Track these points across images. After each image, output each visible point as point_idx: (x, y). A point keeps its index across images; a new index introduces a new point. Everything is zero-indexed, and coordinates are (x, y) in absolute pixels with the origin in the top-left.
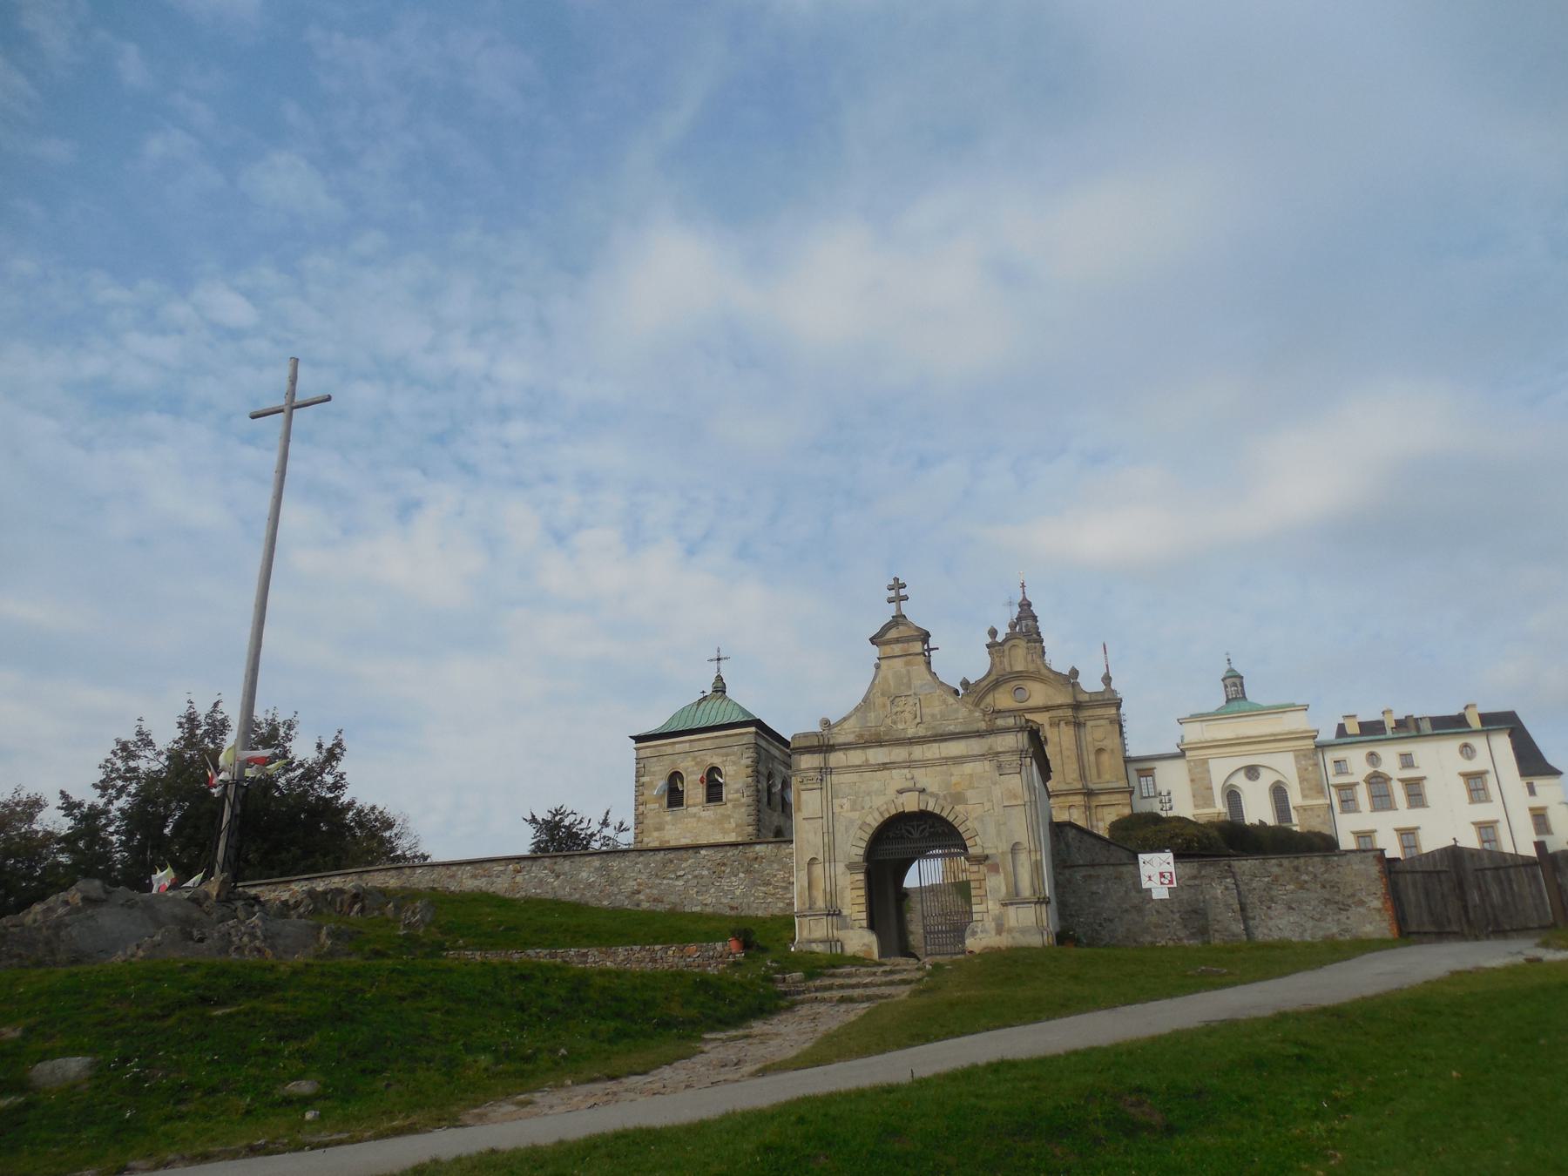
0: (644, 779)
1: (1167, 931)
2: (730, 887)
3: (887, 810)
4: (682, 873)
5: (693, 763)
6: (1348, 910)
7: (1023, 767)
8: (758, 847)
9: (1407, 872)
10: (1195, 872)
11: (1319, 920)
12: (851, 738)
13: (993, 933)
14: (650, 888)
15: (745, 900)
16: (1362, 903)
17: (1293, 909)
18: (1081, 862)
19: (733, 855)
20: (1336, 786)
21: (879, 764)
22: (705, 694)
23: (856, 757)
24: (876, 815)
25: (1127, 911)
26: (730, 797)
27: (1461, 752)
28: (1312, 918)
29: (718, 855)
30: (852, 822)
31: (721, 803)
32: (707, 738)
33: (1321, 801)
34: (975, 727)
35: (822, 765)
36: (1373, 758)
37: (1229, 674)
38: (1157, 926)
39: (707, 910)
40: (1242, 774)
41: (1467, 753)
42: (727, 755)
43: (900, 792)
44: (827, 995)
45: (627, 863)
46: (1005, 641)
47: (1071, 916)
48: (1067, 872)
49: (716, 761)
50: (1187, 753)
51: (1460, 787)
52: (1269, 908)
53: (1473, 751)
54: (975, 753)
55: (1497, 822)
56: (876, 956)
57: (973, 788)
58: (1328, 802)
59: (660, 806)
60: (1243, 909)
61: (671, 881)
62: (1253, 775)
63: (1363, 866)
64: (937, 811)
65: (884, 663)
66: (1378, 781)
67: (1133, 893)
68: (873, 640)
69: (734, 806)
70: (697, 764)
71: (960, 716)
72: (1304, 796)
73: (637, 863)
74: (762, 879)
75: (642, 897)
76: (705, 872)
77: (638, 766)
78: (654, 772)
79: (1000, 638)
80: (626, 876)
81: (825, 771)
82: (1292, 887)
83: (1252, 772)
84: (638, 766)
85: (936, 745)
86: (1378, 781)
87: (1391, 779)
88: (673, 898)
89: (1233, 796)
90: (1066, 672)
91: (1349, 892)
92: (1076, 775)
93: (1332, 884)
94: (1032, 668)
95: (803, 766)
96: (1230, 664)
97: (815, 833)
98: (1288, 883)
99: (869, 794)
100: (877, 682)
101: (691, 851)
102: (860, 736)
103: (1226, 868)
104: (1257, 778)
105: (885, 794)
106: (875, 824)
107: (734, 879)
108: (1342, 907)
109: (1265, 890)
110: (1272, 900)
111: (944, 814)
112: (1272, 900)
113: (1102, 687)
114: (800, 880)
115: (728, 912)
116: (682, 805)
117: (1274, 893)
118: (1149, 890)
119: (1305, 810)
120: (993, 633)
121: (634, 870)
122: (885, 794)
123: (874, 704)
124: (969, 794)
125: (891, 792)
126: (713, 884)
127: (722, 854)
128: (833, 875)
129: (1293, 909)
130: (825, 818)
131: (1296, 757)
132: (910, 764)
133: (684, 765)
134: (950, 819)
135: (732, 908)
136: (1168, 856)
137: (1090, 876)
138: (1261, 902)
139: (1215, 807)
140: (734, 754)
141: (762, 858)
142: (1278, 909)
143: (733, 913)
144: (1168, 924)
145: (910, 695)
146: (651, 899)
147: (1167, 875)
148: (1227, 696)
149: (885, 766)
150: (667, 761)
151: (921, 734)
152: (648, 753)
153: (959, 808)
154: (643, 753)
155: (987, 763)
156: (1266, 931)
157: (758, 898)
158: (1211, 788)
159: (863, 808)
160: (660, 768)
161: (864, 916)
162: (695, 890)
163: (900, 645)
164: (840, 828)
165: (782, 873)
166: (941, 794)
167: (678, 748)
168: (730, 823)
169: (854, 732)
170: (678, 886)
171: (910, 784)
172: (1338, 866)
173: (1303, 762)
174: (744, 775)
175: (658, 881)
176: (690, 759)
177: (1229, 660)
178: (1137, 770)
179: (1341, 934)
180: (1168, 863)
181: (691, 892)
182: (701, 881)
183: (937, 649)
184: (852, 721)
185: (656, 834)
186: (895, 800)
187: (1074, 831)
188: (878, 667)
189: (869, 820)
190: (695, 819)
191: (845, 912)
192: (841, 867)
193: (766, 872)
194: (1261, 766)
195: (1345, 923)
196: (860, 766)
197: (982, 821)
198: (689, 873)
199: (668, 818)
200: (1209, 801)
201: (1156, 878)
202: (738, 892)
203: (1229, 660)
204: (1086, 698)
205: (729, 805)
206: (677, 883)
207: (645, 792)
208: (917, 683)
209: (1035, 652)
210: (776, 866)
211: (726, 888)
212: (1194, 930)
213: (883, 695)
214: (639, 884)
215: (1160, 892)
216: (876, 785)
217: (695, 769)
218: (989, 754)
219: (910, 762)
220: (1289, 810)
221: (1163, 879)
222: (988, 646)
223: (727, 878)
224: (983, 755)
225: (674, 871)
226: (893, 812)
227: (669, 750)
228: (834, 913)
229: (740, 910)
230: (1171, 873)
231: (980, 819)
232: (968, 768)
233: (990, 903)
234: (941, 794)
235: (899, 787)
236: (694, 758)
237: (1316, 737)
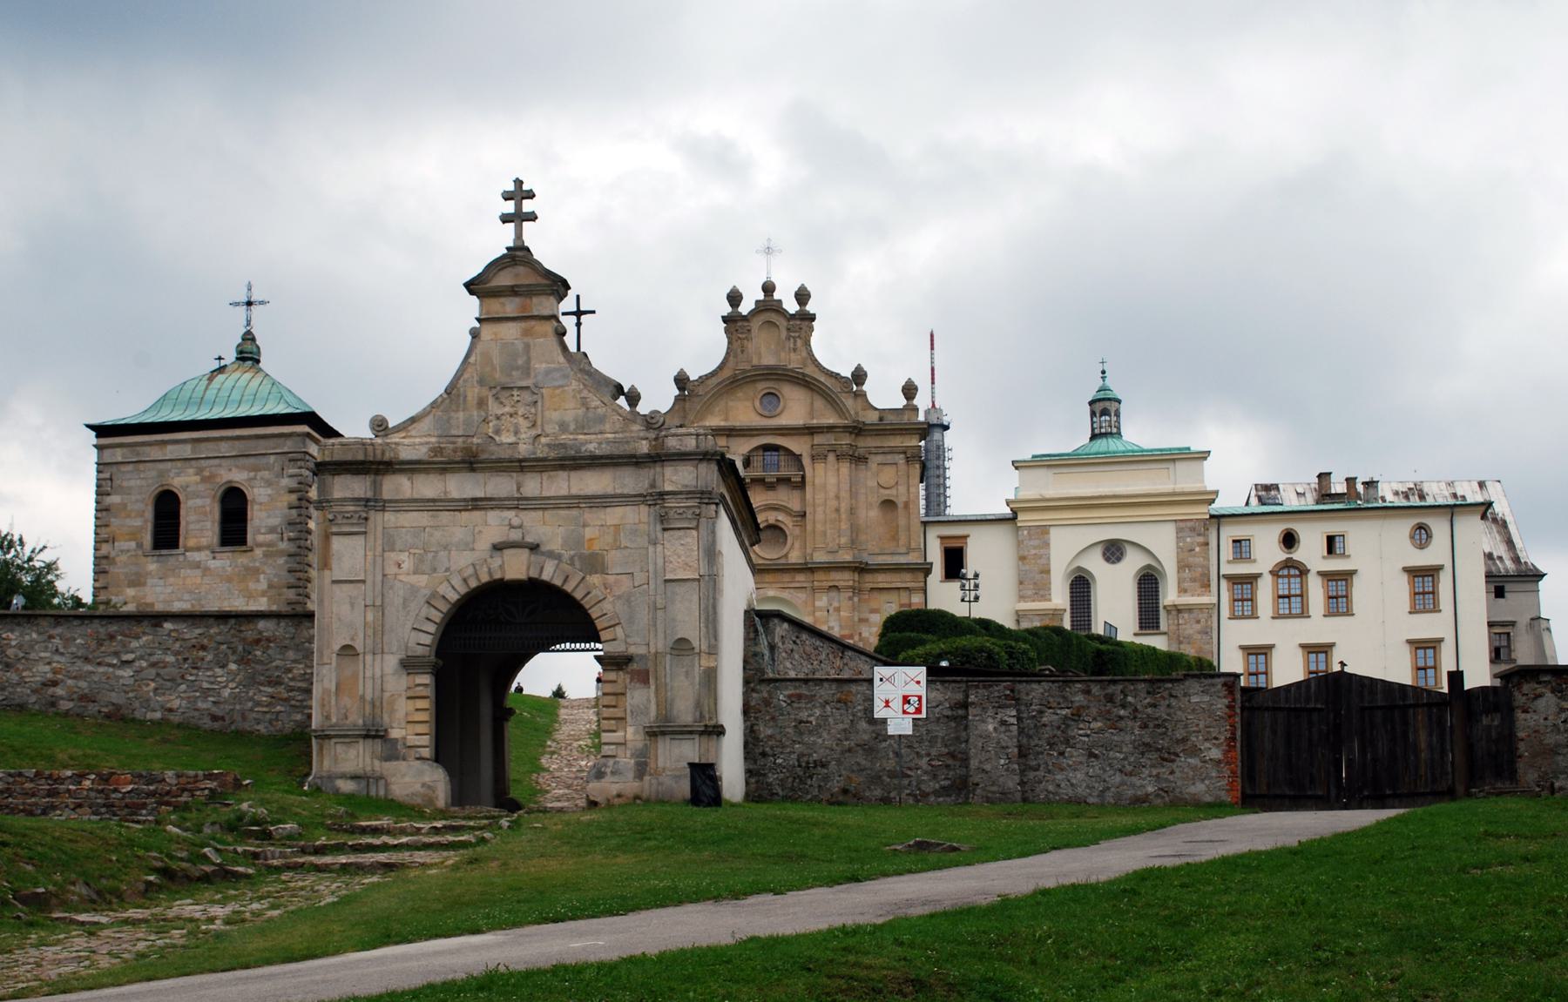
0: (115, 499)
1: (906, 782)
2: (212, 683)
3: (476, 575)
4: (130, 657)
5: (198, 478)
6: (1173, 761)
7: (703, 520)
8: (262, 624)
9: (1267, 709)
10: (960, 696)
11: (1131, 774)
12: (420, 453)
13: (631, 775)
14: (75, 678)
15: (238, 707)
16: (1195, 751)
17: (1096, 756)
18: (792, 674)
19: (220, 634)
20: (1229, 578)
21: (465, 500)
23: (428, 486)
24: (457, 582)
25: (850, 750)
26: (261, 538)
27: (1412, 537)
28: (1121, 771)
29: (192, 633)
30: (414, 590)
31: (244, 548)
32: (221, 439)
33: (1205, 600)
34: (628, 449)
35: (369, 495)
36: (1289, 540)
37: (1101, 394)
38: (892, 775)
39: (172, 718)
40: (1098, 552)
41: (1421, 539)
42: (256, 469)
43: (498, 548)
44: (327, 859)
45: (34, 636)
46: (753, 313)
47: (764, 754)
48: (764, 690)
51: (1401, 589)
52: (1062, 754)
53: (1429, 536)
54: (626, 491)
55: (1440, 641)
56: (441, 803)
57: (619, 548)
58: (1215, 600)
59: (140, 546)
60: (1023, 753)
61: (111, 670)
62: (1113, 554)
63: (1206, 698)
64: (558, 582)
65: (488, 332)
66: (1291, 569)
67: (863, 725)
68: (472, 286)
69: (266, 555)
70: (204, 480)
71: (607, 427)
72: (1182, 590)
73: (51, 637)
74: (268, 673)
75: (59, 691)
76: (170, 659)
77: (102, 476)
78: (130, 488)
79: (746, 307)
80: (33, 656)
81: (373, 503)
82: (1099, 724)
83: (1114, 551)
84: (102, 476)
85: (563, 474)
86: (1291, 569)
87: (1309, 571)
88: (114, 697)
89: (1081, 586)
90: (847, 373)
91: (1179, 735)
92: (843, 540)
93: (1160, 722)
94: (793, 362)
95: (337, 494)
96: (1103, 378)
97: (352, 605)
98: (1095, 719)
99: (445, 548)
100: (472, 360)
101: (146, 623)
102: (437, 450)
103: (1008, 692)
104: (1119, 559)
105: (473, 549)
106: (453, 597)
107: (219, 671)
108: (1166, 755)
109: (1059, 728)
110: (1067, 742)
111: (568, 588)
112: (1067, 742)
113: (900, 402)
114: (325, 679)
115: (207, 723)
116: (176, 546)
117: (1073, 732)
118: (884, 721)
119: (1179, 611)
120: (734, 298)
121: (47, 647)
122: (473, 549)
123: (466, 397)
124: (613, 558)
125: (484, 544)
126: (183, 677)
127: (198, 631)
128: (378, 673)
129: (1096, 756)
130: (369, 582)
131: (1179, 531)
132: (519, 503)
133: (180, 481)
134: (578, 595)
135: (214, 718)
136: (920, 672)
137: (799, 697)
138: (1051, 745)
139: (1050, 600)
140: (267, 468)
141: (268, 640)
142: (1075, 755)
143: (217, 725)
144: (909, 772)
145: (527, 388)
146: (75, 696)
147: (913, 700)
148: (1093, 429)
149: (475, 504)
150: (151, 472)
151: (539, 455)
152: (118, 455)
153: (595, 579)
154: (109, 456)
155: (644, 509)
156: (1051, 788)
157: (258, 704)
158: (1048, 572)
159: (435, 570)
160: (138, 482)
161: (425, 740)
162: (153, 685)
163: (517, 300)
164: (396, 598)
165: (301, 666)
166: (566, 555)
167: (172, 451)
168: (258, 581)
169: (427, 443)
170: (122, 677)
171: (515, 536)
172: (1171, 696)
173: (1188, 540)
174: (286, 504)
175: (90, 668)
176: (191, 471)
177: (1103, 372)
178: (942, 538)
179: (1158, 796)
180: (918, 682)
181: (145, 689)
182: (162, 672)
183: (593, 312)
184: (425, 425)
185: (131, 592)
186: (489, 560)
187: (786, 625)
188: (475, 334)
189: (444, 589)
190: (198, 572)
191: (395, 733)
192: (392, 662)
193: (274, 664)
195: (1167, 780)
196: (434, 500)
197: (628, 601)
198: (141, 658)
199: (152, 566)
200: (1042, 591)
201: (897, 704)
202: (226, 693)
203: (1103, 372)
204: (872, 418)
205: (258, 552)
206: (120, 673)
207: (113, 520)
208: (539, 366)
210: (291, 654)
211: (205, 685)
212: (946, 783)
213: (481, 382)
214: (55, 672)
215: (900, 725)
216: (459, 534)
217: (201, 487)
218: (651, 495)
219: (518, 499)
220: (1158, 611)
221: (906, 706)
222: (725, 319)
223: (208, 669)
224: (640, 495)
225: (116, 654)
226: (485, 578)
227: (155, 453)
228: (374, 733)
229: (227, 722)
230: (920, 698)
231: (627, 599)
232: (614, 515)
233: (630, 730)
234: (566, 555)
235: (498, 539)
236: (199, 471)
237: (1213, 501)
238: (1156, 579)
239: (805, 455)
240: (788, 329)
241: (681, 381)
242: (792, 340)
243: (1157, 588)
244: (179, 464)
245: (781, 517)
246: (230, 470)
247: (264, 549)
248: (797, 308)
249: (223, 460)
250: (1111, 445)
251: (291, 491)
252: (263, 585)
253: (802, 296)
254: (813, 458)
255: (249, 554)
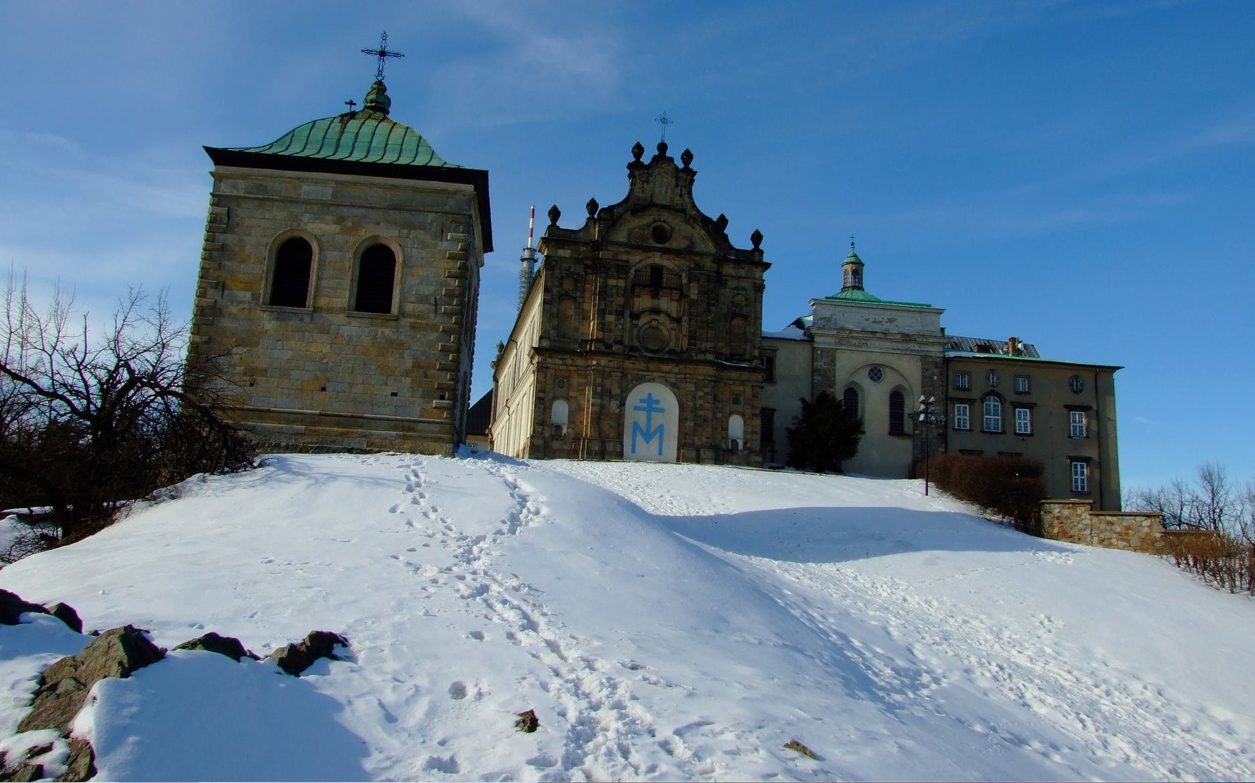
0: (229, 239)
22: (354, 108)
40: (867, 370)
42: (410, 226)
49: (389, 236)
50: (816, 339)
59: (255, 298)
62: (875, 374)
79: (646, 159)
83: (876, 373)
104: (879, 379)
113: (749, 246)
120: (638, 151)
133: (315, 228)
140: (423, 227)
154: (225, 189)
176: (329, 218)
194: (887, 366)
203: (853, 244)
209: (685, 187)
222: (630, 166)
238: (902, 396)
239: (684, 275)
240: (677, 179)
241: (592, 205)
242: (679, 188)
243: (903, 402)
244: (316, 208)
245: (662, 318)
246: (379, 223)
247: (412, 320)
248: (683, 166)
249: (370, 210)
250: (857, 294)
251: (452, 257)
252: (409, 363)
253: (687, 156)
254: (690, 279)
255: (393, 324)
